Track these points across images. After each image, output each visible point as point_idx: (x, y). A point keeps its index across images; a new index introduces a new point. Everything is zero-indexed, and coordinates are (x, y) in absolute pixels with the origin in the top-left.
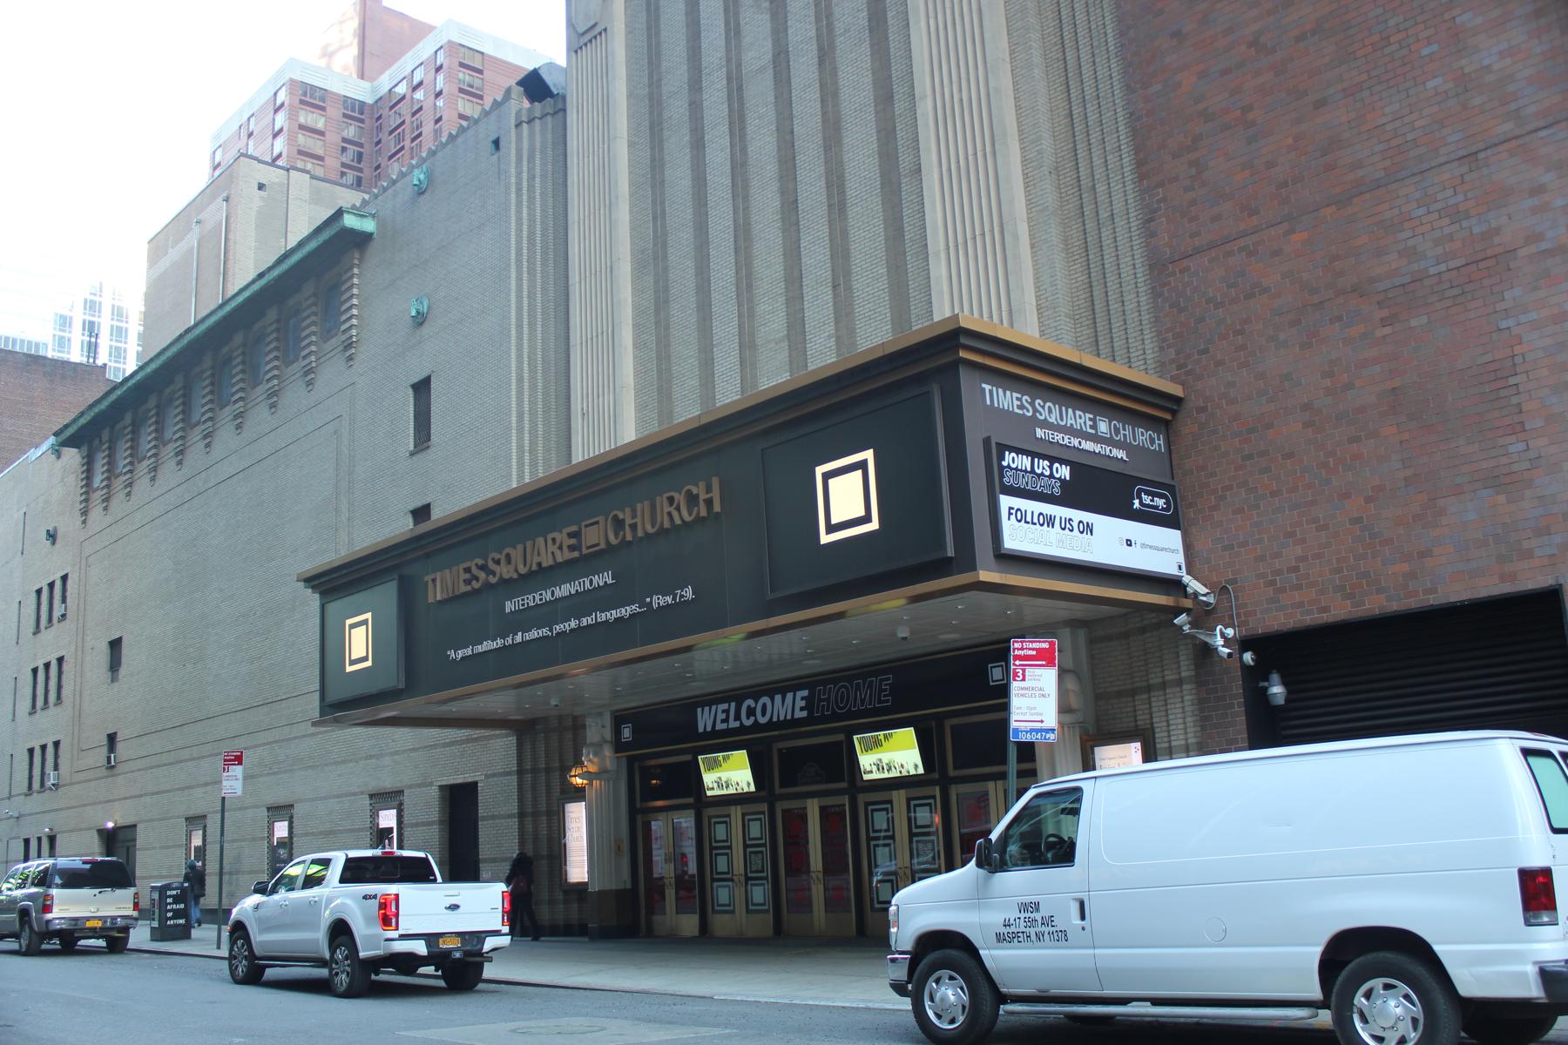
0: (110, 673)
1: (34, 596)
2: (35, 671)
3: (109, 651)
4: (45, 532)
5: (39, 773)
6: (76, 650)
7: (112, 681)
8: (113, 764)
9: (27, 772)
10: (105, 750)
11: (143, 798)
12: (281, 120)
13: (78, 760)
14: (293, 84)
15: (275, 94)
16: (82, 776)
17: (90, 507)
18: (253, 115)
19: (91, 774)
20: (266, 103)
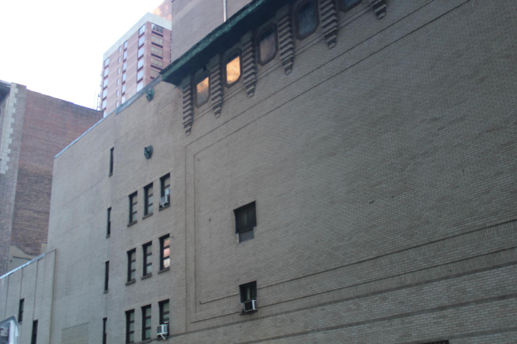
0: (238, 235)
1: (128, 199)
2: (131, 253)
3: (234, 217)
4: (143, 150)
5: (141, 328)
6: (186, 226)
7: (240, 241)
8: (254, 308)
9: (125, 329)
10: (239, 298)
11: (310, 335)
12: (142, 40)
13: (196, 312)
14: (148, 24)
15: (139, 30)
16: (198, 326)
17: (195, 118)
18: (127, 41)
19: (219, 322)
20: (134, 35)
